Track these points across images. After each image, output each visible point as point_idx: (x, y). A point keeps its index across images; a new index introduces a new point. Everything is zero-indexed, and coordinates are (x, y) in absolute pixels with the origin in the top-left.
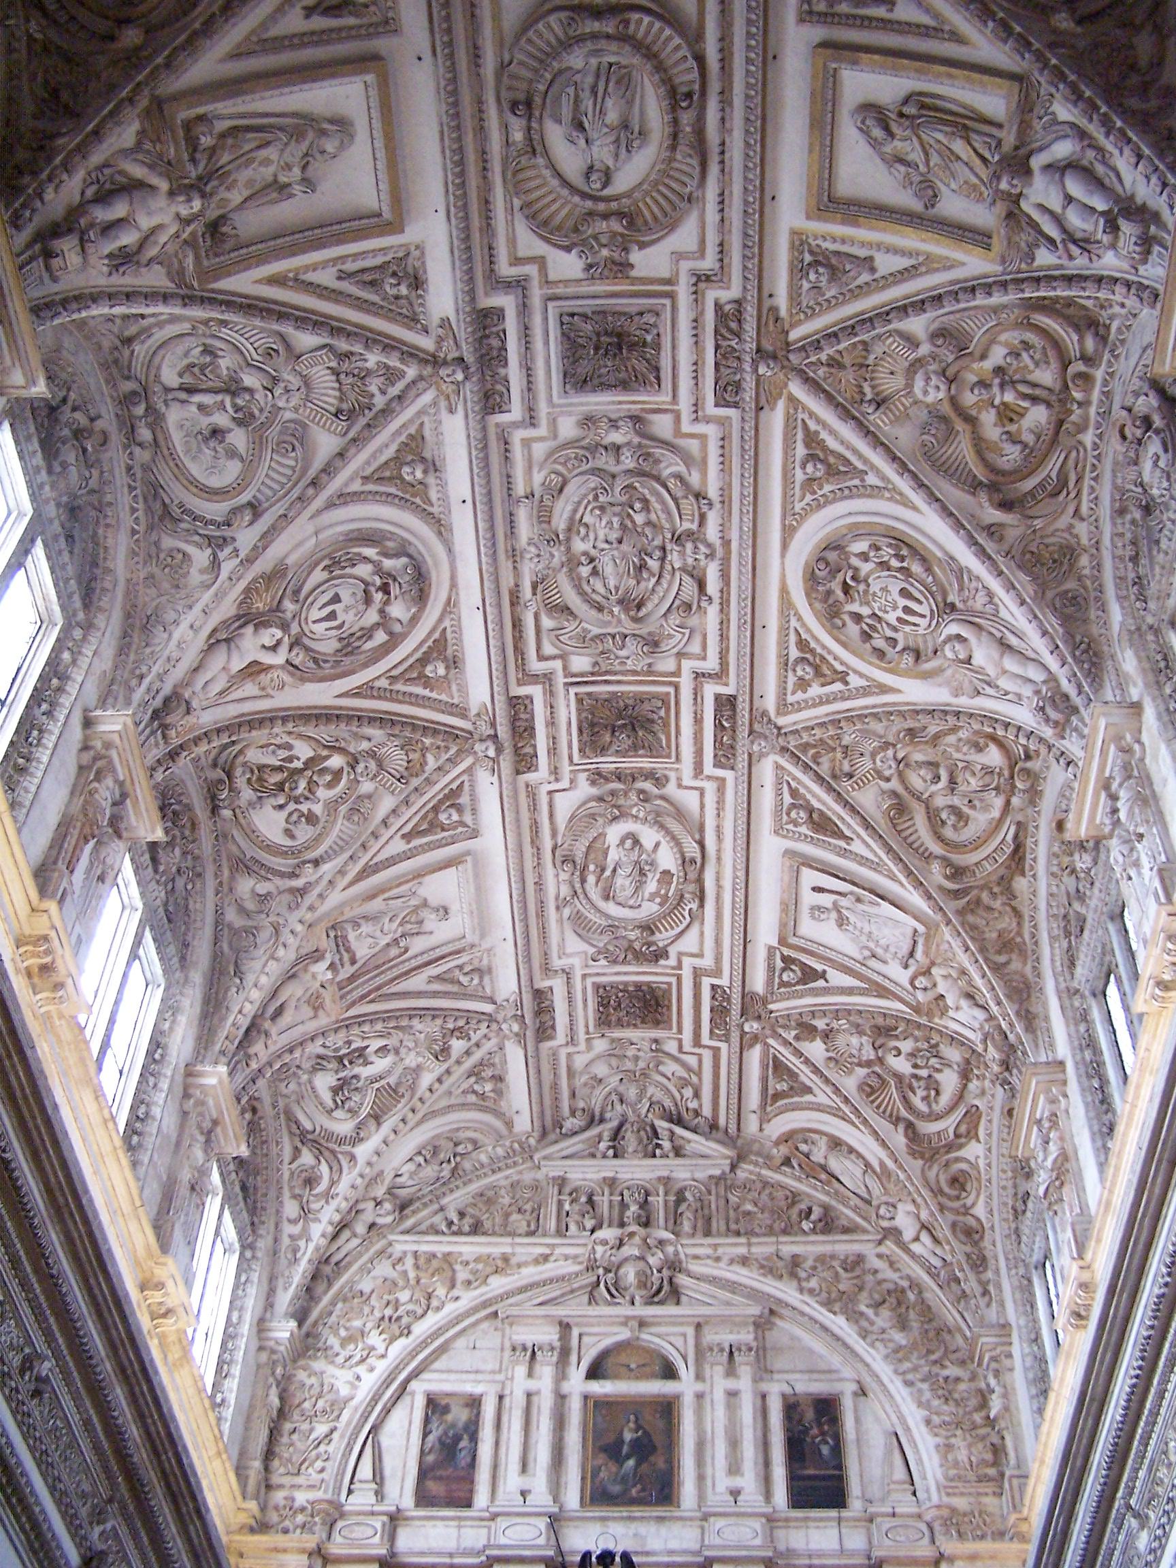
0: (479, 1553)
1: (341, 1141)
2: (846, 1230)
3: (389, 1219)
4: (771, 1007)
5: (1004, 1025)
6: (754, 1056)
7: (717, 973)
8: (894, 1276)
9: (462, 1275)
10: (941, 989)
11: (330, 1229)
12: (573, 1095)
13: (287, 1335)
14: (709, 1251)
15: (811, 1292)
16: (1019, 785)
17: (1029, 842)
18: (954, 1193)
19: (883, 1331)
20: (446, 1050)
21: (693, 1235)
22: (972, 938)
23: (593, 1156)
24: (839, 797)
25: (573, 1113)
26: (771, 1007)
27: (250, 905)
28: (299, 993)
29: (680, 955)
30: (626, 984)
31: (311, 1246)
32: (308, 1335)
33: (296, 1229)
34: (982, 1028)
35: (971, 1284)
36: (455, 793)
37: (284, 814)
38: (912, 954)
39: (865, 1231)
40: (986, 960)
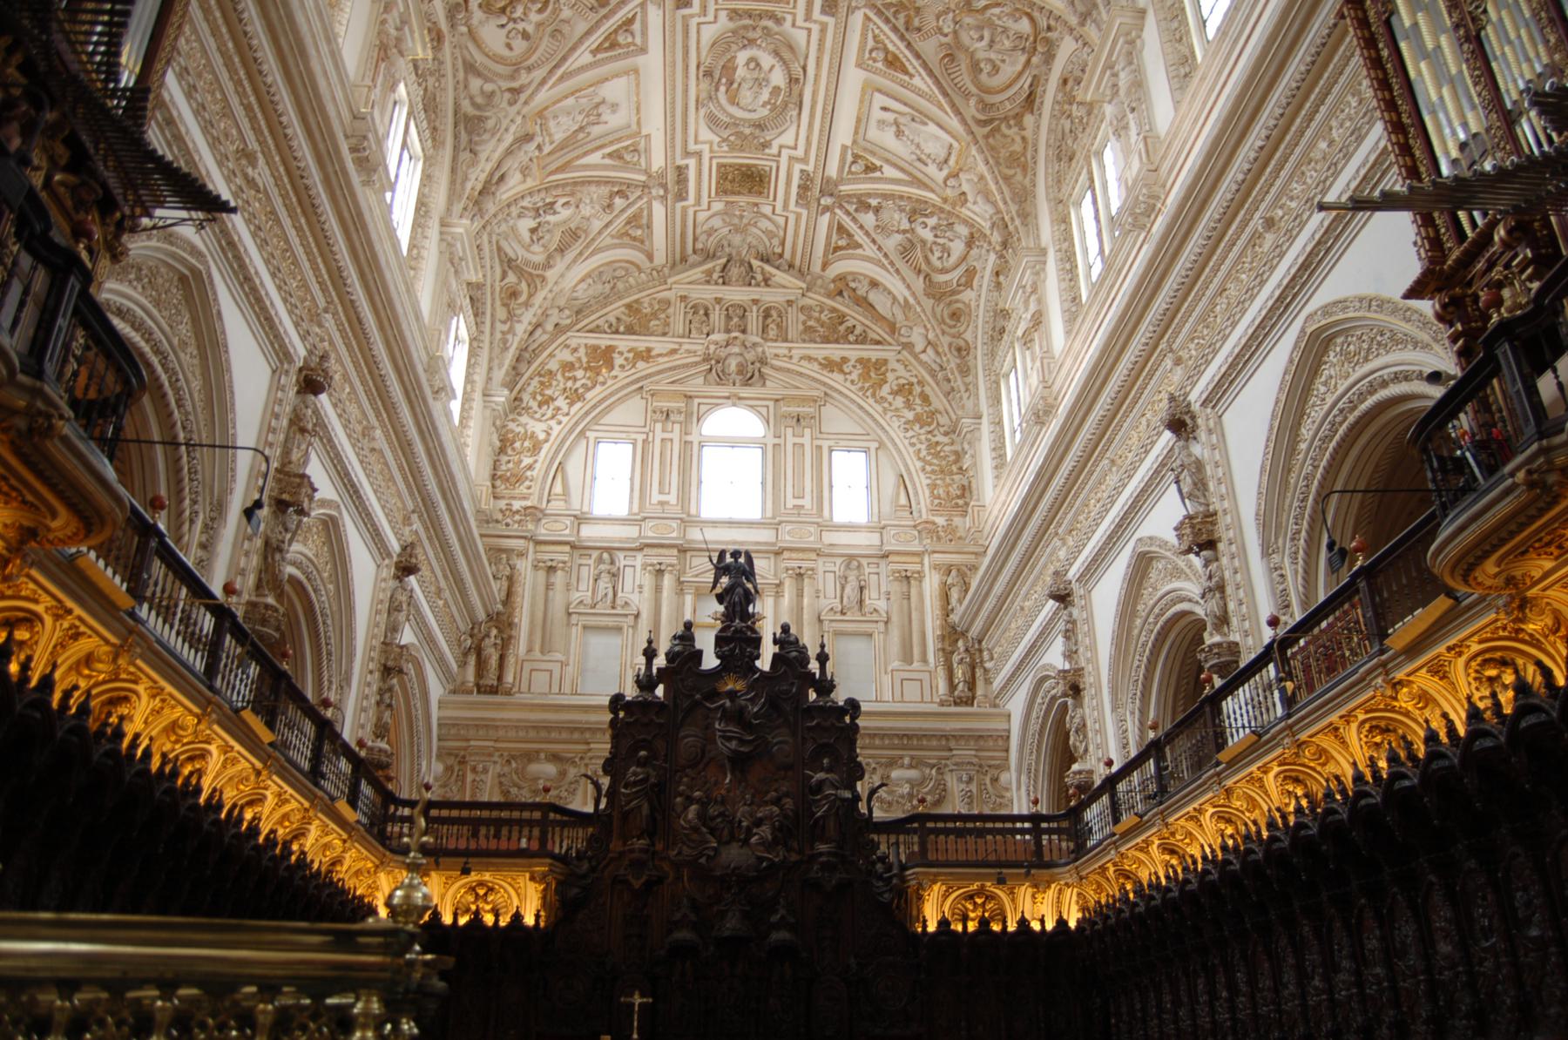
0: (635, 540)
1: (536, 267)
2: (878, 343)
3: (569, 321)
4: (842, 188)
5: (1006, 218)
6: (825, 220)
7: (805, 160)
8: (907, 375)
9: (619, 361)
10: (965, 187)
11: (530, 328)
12: (695, 239)
13: (503, 399)
14: (786, 352)
15: (852, 382)
16: (1040, 49)
17: (1040, 89)
18: (953, 323)
19: (897, 410)
20: (609, 206)
21: (776, 341)
22: (993, 157)
23: (708, 282)
24: (909, 45)
25: (695, 252)
26: (842, 188)
27: (479, 100)
28: (516, 165)
29: (781, 147)
30: (741, 165)
31: (517, 339)
32: (515, 399)
33: (506, 327)
34: (991, 218)
35: (958, 383)
36: (630, 21)
37: (505, 31)
38: (946, 161)
39: (890, 344)
40: (1000, 172)
